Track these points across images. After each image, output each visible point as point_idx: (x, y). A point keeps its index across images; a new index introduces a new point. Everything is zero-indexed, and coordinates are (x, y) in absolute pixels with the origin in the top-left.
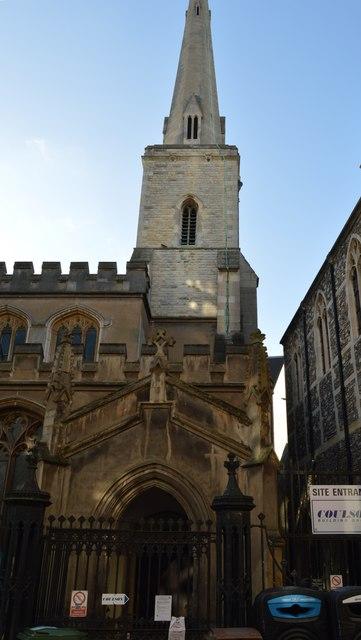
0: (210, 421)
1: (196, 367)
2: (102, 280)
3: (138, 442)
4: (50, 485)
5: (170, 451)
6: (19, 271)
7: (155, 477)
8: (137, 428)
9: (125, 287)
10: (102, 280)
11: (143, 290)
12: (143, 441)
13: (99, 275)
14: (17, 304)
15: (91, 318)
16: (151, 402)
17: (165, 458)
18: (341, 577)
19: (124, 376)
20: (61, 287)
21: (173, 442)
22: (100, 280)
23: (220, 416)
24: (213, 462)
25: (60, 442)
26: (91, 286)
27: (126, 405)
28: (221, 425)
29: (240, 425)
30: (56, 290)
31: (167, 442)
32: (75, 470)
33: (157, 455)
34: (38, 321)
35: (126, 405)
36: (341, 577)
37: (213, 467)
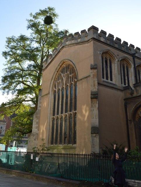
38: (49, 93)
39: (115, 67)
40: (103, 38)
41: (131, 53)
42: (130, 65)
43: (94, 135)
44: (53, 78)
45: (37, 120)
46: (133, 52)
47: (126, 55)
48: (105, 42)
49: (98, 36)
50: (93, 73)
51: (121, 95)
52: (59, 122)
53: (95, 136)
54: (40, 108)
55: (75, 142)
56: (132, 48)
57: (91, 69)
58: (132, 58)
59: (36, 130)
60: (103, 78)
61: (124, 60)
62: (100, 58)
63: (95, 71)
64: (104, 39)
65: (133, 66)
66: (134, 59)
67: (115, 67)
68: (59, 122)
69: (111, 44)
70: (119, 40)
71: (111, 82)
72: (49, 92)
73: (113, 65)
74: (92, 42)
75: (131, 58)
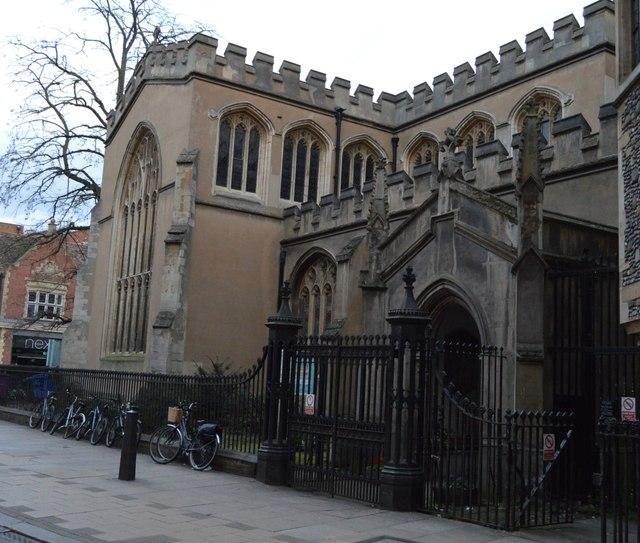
0: (486, 225)
1: (568, 146)
2: (560, 44)
3: (432, 260)
4: (371, 309)
5: (455, 264)
6: (481, 67)
7: (450, 293)
8: (432, 244)
9: (585, 44)
10: (560, 44)
11: (344, 124)
12: (436, 255)
13: (556, 40)
14: (481, 107)
15: (553, 98)
16: (439, 214)
17: (451, 273)
18: (634, 400)
19: (498, 178)
20: (521, 71)
21: (458, 254)
22: (557, 46)
23: (494, 218)
24: (488, 267)
25: (378, 266)
26: (549, 58)
27: (422, 226)
28: (494, 228)
29: (510, 224)
30: (514, 77)
31: (452, 254)
32: (391, 294)
33: (446, 270)
34: (502, 122)
35: (422, 226)
36: (634, 400)
37: (489, 277)
38: (110, 218)
39: (269, 154)
40: (234, 67)
41: (332, 109)
42: (323, 142)
43: (160, 331)
44: (123, 172)
45: (87, 289)
46: (340, 102)
47: (312, 116)
48: (237, 80)
49: (212, 63)
50: (183, 176)
51: (275, 231)
52: (129, 295)
53: (162, 334)
54: (94, 255)
55: (142, 347)
56: (339, 91)
57: (179, 163)
58: (333, 120)
59: (84, 313)
60: (221, 181)
61: (306, 128)
62: (215, 130)
63: (189, 169)
64: (235, 72)
65: (331, 146)
66: (338, 125)
67: (269, 154)
68: (129, 295)
69: (261, 85)
70: (291, 69)
71: (249, 195)
72: (112, 212)
73: (262, 145)
74: (191, 84)
75: (327, 123)
